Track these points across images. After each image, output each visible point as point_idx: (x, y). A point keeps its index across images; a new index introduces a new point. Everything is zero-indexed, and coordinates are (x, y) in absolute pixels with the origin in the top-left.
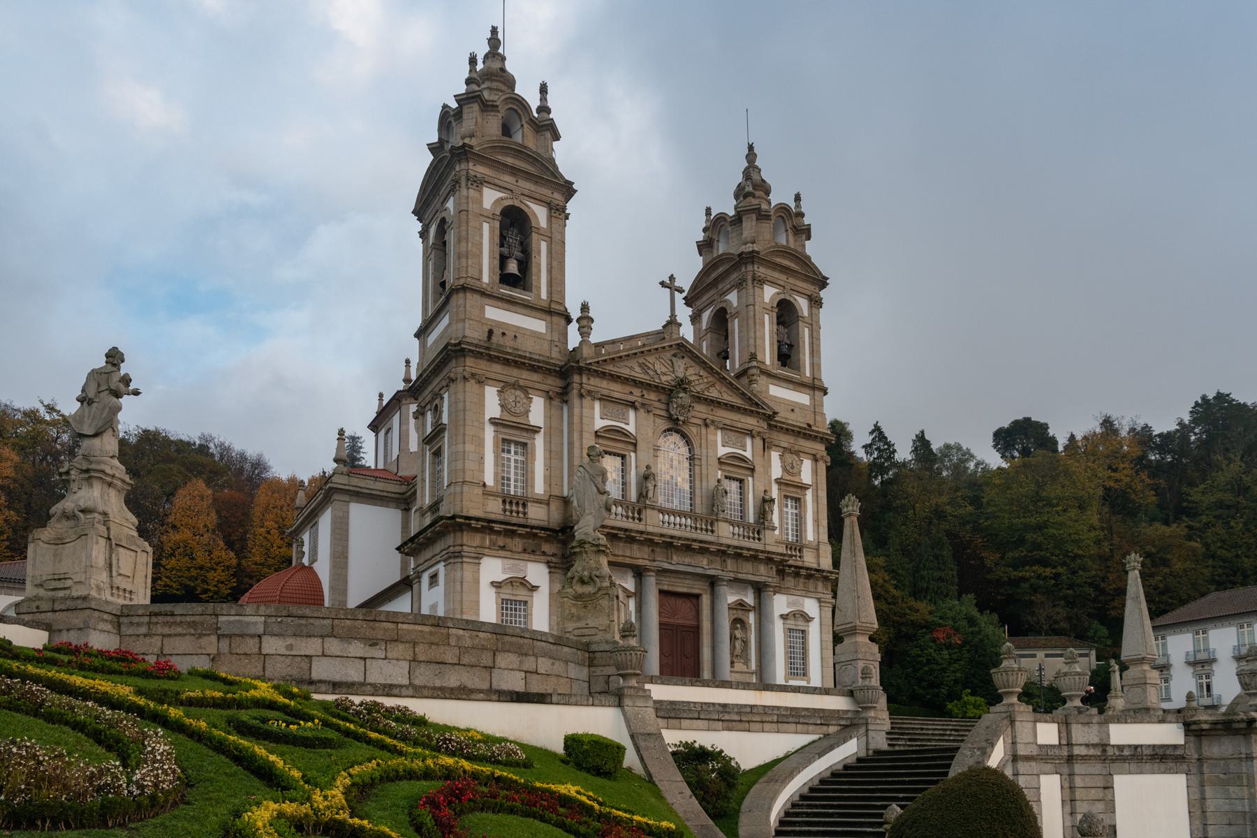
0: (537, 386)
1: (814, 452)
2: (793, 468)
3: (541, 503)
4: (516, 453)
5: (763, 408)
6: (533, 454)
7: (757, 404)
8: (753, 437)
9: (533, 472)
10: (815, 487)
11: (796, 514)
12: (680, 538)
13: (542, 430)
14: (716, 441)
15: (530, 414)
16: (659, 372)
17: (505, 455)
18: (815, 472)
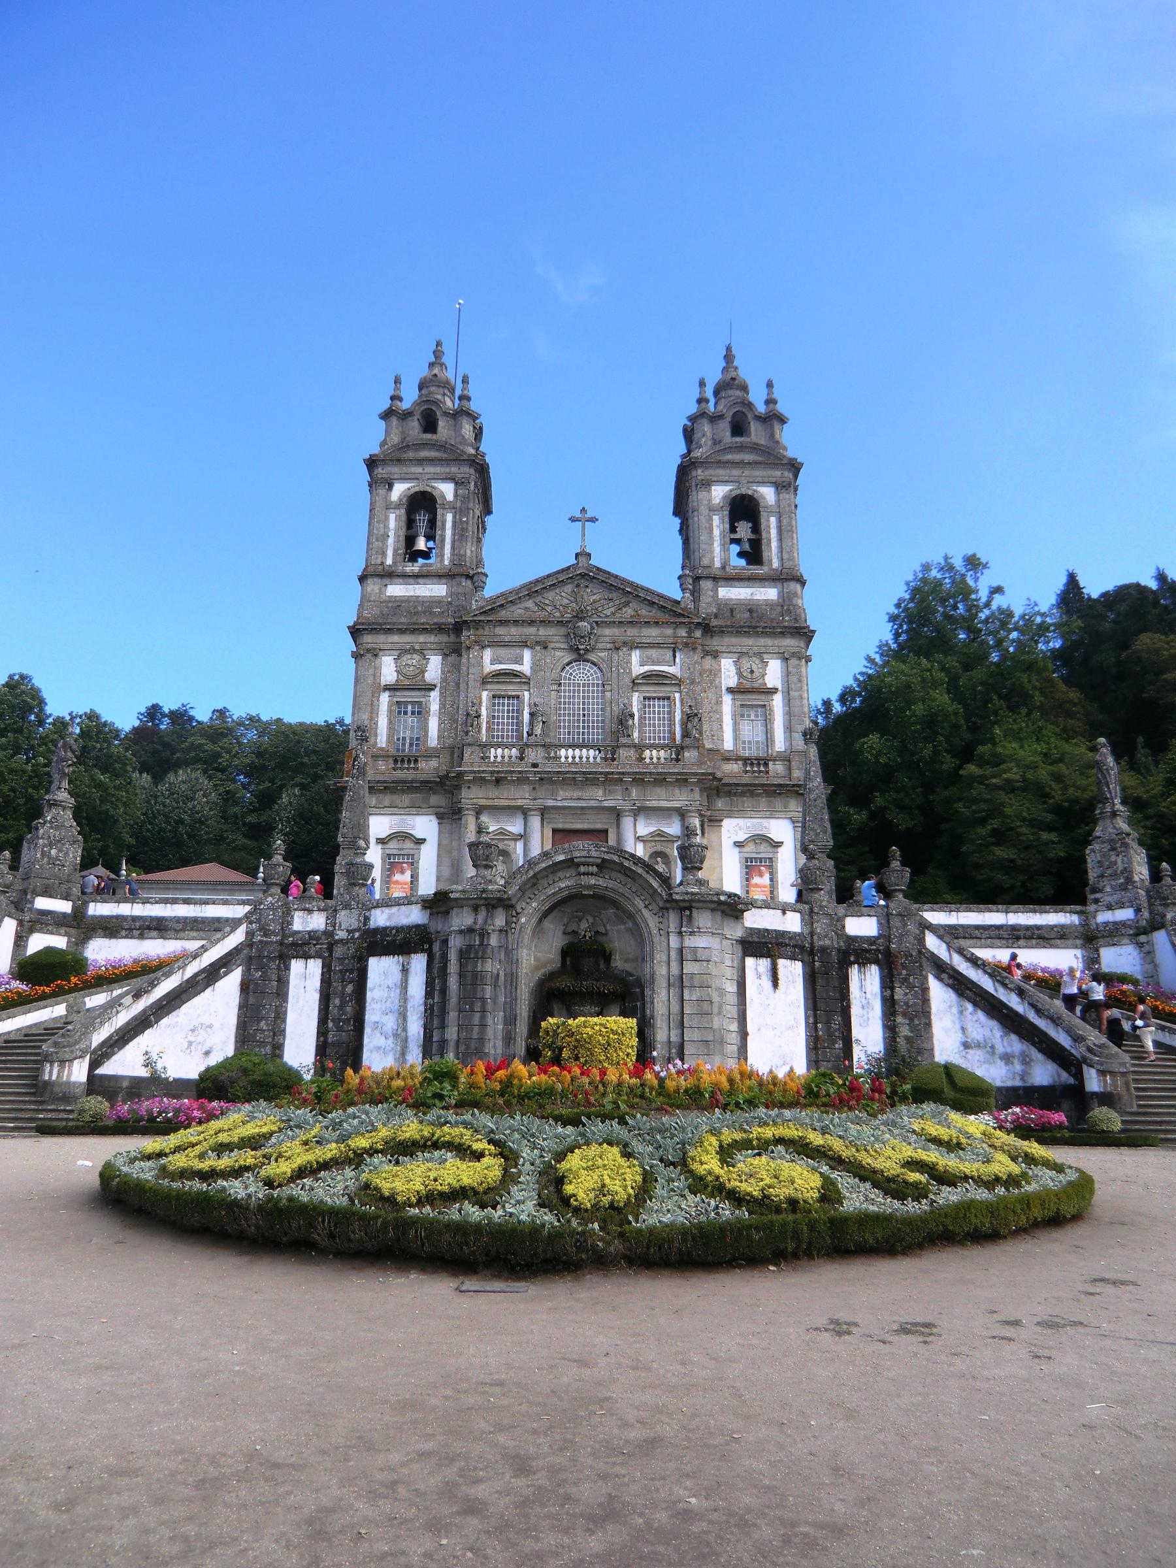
2: (752, 672)
7: (683, 616)
10: (785, 690)
13: (438, 689)
15: (426, 675)
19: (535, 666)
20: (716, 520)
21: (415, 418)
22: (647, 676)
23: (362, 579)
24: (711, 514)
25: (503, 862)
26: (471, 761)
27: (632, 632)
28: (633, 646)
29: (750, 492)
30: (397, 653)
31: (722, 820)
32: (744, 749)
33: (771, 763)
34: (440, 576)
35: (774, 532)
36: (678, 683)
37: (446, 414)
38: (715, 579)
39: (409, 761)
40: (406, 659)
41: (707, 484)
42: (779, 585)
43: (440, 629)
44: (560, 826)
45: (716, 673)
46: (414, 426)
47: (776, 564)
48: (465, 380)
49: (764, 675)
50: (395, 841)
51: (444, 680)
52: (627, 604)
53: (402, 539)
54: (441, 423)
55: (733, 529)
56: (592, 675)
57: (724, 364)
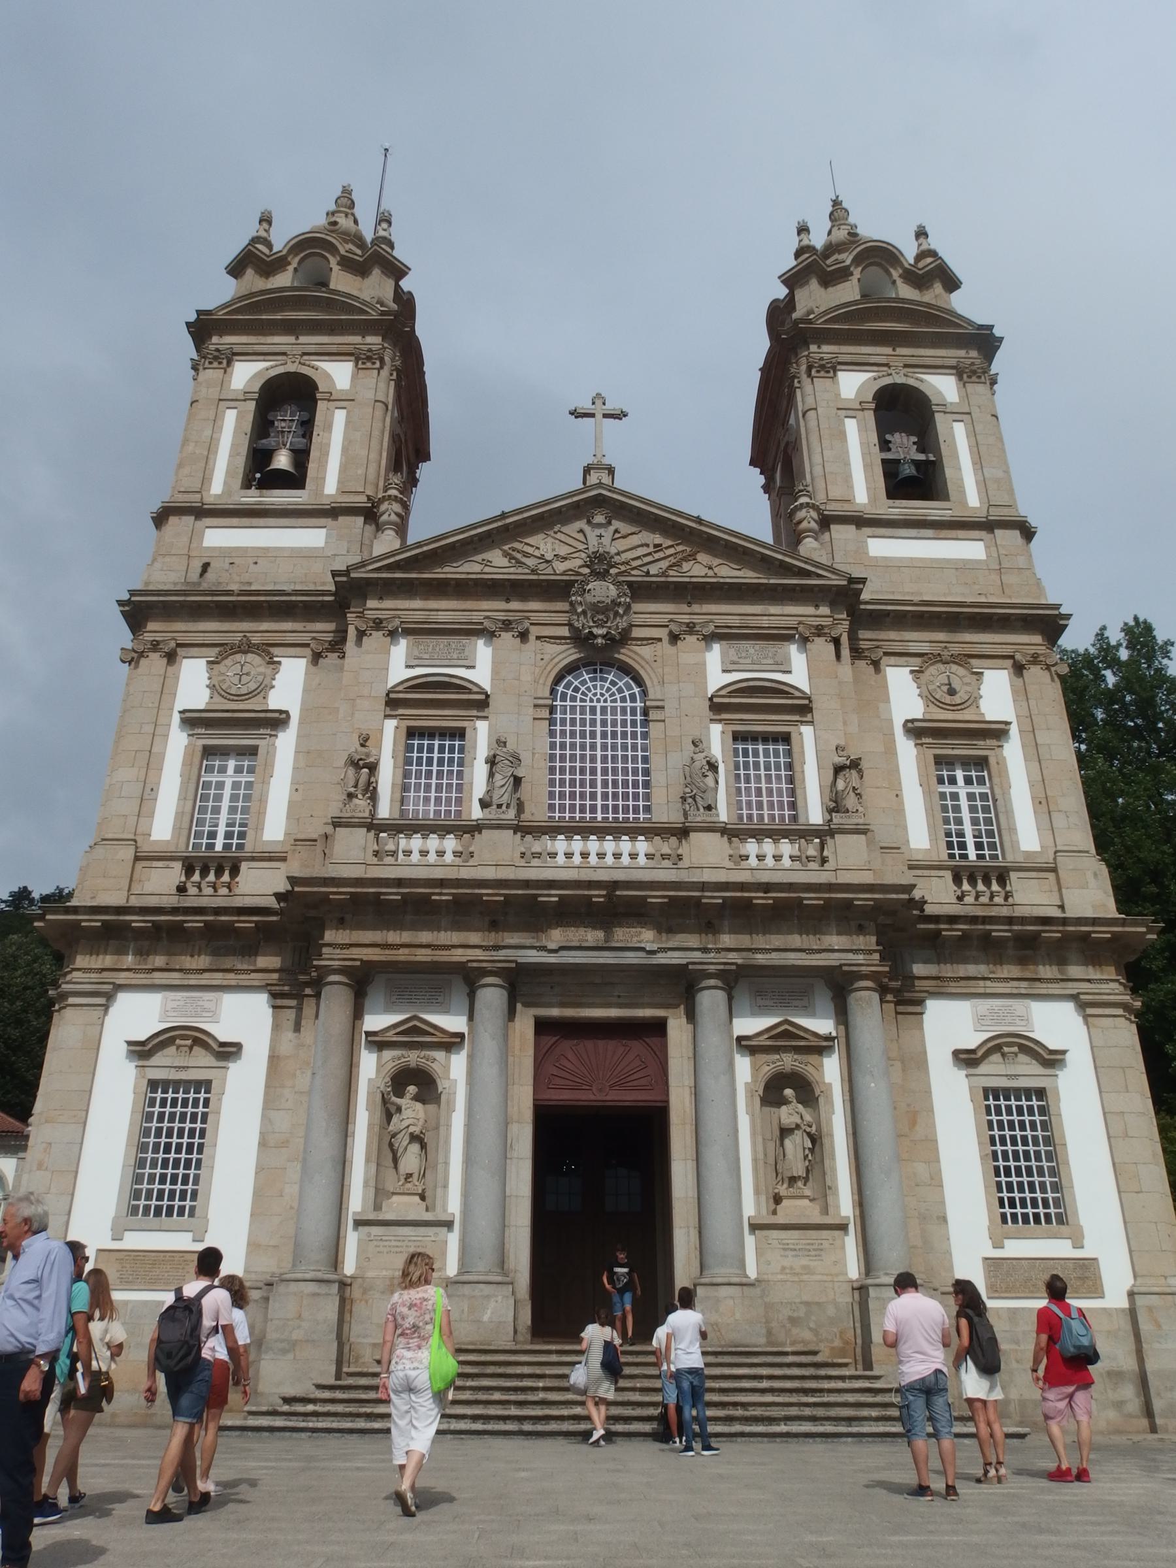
0: (290, 638)
1: (1008, 650)
2: (952, 692)
3: (270, 859)
4: (238, 770)
5: (819, 576)
6: (269, 765)
7: (807, 574)
8: (805, 640)
9: (263, 801)
11: (984, 797)
12: (551, 884)
14: (703, 664)
16: (549, 557)
17: (214, 778)
18: (1021, 695)
20: (851, 426)
21: (291, 268)
23: (161, 518)
24: (843, 413)
25: (417, 1098)
29: (911, 382)
30: (217, 650)
31: (920, 1002)
32: (950, 845)
33: (1013, 875)
38: (860, 521)
39: (219, 872)
42: (983, 534)
44: (555, 1012)
47: (973, 499)
48: (385, 219)
49: (973, 700)
50: (172, 1050)
52: (691, 557)
53: (244, 450)
55: (885, 445)
56: (620, 690)
57: (829, 224)
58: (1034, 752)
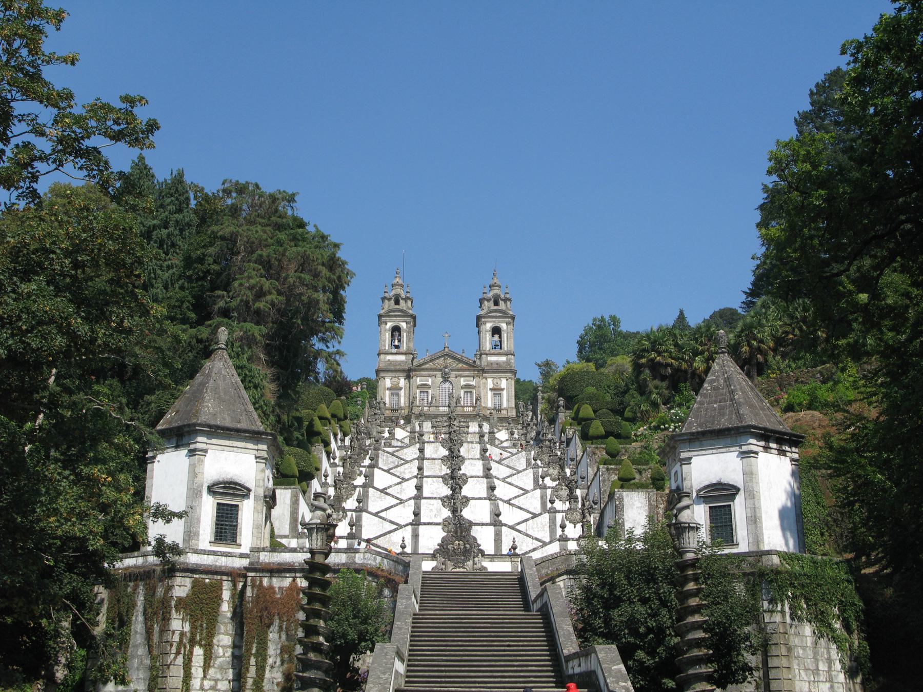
19: (432, 382)
20: (488, 335)
22: (466, 385)
26: (416, 411)
27: (460, 373)
28: (461, 376)
34: (402, 354)
35: (505, 338)
36: (474, 387)
37: (402, 299)
38: (487, 354)
40: (393, 379)
41: (485, 323)
43: (403, 371)
45: (486, 384)
46: (392, 302)
47: (506, 349)
51: (405, 386)
54: (401, 301)
58: (508, 392)
